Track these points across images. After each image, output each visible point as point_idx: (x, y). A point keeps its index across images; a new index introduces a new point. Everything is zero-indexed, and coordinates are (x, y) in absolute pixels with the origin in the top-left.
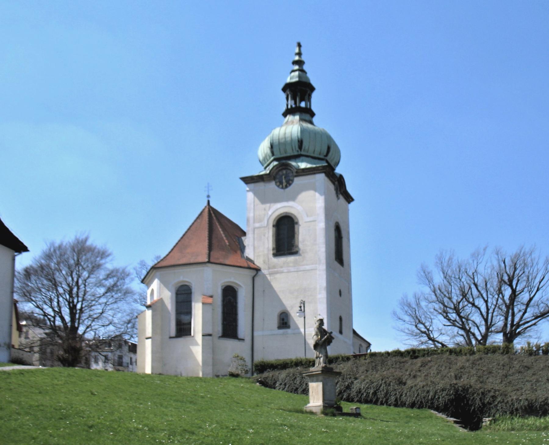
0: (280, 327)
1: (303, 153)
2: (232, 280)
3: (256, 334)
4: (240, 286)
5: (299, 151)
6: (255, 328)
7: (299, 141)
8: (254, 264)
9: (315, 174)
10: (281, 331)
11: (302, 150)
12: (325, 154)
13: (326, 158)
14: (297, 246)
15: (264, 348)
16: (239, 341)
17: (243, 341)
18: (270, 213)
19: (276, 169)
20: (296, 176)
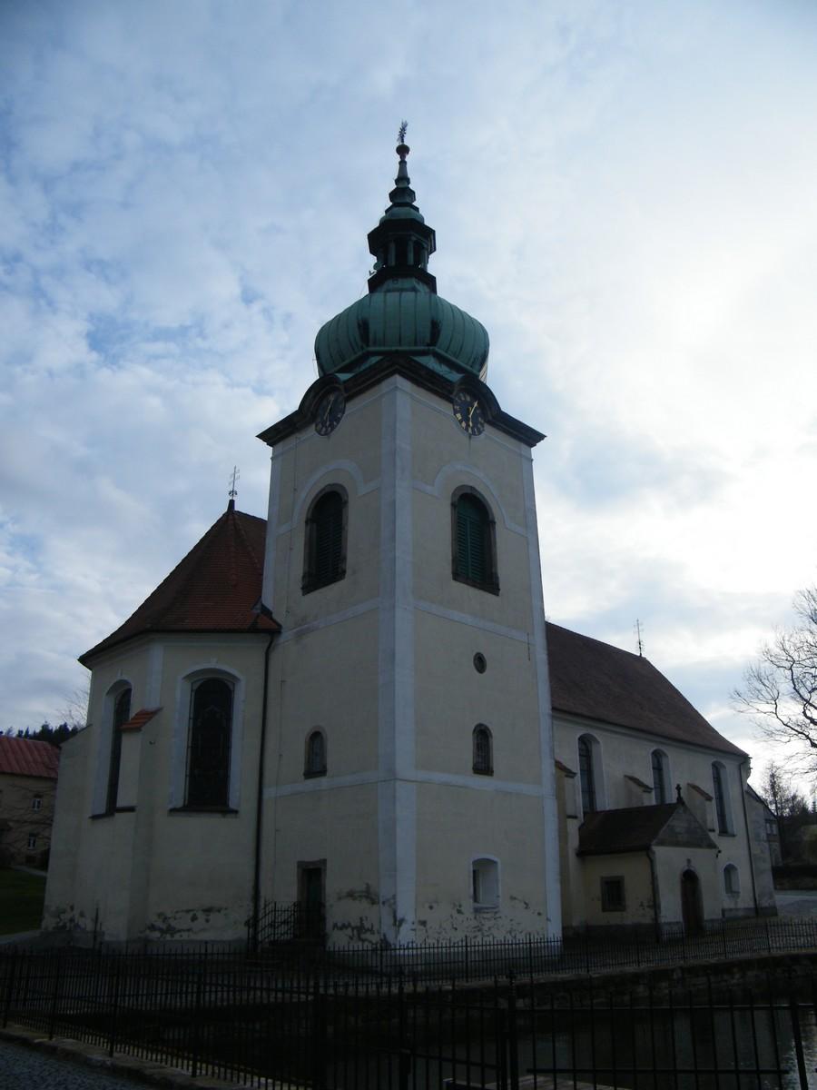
0: (309, 774)
1: (372, 349)
2: (213, 663)
3: (269, 793)
4: (234, 677)
5: (364, 346)
6: (267, 780)
7: (359, 325)
8: (272, 619)
9: (379, 382)
10: (311, 784)
11: (371, 343)
12: (428, 340)
13: (431, 348)
14: (344, 559)
15: (277, 830)
16: (224, 817)
17: (233, 815)
18: (303, 495)
19: (314, 397)
20: (348, 399)
